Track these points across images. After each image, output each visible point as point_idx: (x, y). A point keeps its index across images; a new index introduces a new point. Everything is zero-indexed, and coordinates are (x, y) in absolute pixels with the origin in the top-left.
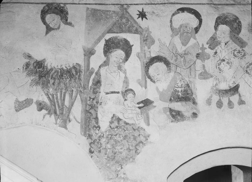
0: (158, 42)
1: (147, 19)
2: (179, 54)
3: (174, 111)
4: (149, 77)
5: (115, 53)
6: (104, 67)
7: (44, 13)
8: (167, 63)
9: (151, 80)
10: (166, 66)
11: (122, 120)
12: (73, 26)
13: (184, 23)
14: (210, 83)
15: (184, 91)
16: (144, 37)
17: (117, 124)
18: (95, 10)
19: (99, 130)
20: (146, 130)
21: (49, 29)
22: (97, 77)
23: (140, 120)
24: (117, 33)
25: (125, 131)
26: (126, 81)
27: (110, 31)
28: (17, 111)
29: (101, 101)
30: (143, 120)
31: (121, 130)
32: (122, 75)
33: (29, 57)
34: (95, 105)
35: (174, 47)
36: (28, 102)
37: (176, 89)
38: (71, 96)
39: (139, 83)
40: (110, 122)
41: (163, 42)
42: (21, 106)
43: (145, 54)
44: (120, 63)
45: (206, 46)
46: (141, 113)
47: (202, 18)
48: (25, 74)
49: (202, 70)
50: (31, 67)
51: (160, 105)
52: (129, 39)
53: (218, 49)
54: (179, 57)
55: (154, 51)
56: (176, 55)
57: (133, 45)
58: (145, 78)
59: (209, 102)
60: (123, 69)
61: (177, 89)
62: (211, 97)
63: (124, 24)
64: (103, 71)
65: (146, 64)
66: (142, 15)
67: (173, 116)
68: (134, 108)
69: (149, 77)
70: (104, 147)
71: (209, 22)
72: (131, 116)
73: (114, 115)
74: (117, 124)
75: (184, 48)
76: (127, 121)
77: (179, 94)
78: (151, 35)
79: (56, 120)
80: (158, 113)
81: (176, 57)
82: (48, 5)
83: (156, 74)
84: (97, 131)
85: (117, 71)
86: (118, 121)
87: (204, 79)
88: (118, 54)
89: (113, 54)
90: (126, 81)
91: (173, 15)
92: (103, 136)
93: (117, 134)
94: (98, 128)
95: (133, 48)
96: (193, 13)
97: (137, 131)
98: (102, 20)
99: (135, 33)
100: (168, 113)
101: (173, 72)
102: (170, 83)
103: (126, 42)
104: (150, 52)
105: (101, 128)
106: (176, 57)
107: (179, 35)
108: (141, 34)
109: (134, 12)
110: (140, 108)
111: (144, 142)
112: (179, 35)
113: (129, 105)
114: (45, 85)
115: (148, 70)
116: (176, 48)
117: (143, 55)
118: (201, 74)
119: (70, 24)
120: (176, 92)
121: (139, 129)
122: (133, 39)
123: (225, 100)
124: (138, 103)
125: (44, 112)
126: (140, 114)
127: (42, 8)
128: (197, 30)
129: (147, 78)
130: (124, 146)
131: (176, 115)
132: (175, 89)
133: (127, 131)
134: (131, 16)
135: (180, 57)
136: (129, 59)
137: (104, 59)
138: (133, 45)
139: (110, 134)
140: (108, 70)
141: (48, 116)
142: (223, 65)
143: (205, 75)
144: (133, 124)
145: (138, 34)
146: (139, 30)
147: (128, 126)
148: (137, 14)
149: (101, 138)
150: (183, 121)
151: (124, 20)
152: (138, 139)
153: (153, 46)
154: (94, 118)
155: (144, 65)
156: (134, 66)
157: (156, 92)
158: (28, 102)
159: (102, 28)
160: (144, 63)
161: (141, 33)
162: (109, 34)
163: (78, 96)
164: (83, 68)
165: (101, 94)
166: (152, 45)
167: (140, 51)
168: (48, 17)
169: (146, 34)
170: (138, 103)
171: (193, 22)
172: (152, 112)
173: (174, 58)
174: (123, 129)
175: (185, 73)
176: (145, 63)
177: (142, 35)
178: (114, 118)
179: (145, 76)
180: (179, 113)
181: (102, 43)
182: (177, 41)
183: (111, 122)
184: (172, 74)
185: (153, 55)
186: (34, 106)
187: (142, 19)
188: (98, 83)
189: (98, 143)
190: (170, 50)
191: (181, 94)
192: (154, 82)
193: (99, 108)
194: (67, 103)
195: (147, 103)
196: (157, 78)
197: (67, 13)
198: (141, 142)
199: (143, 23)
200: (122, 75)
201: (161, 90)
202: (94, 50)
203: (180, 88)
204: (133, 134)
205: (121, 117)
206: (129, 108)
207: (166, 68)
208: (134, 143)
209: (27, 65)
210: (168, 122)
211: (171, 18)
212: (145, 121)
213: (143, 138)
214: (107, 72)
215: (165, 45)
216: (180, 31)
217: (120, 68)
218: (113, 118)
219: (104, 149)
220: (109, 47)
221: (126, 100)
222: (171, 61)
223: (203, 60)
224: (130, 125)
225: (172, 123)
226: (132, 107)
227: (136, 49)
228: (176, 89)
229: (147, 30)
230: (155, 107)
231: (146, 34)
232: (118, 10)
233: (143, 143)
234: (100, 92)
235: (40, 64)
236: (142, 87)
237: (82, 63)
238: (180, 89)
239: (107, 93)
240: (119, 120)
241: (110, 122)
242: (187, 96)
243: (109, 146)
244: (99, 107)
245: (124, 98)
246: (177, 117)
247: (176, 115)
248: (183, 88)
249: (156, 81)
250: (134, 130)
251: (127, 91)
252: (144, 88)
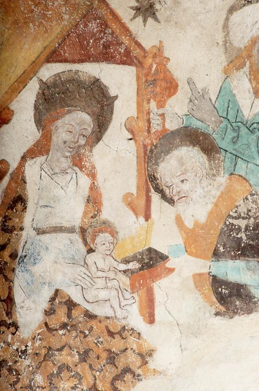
0: (187, 87)
1: (156, 20)
2: (245, 123)
3: (227, 284)
4: (158, 190)
5: (67, 118)
6: (35, 160)
8: (209, 148)
9: (164, 197)
10: (205, 157)
11: (79, 305)
15: (254, 229)
16: (147, 75)
17: (65, 320)
19: (13, 334)
20: (143, 335)
22: (13, 185)
23: (128, 308)
24: (74, 62)
25: (85, 336)
26: (94, 200)
27: (54, 56)
29: (24, 254)
30: (135, 309)
31: (74, 334)
32: (85, 181)
34: (6, 263)
35: (232, 102)
37: (231, 221)
40: (45, 311)
41: (200, 86)
43: (149, 121)
44: (79, 146)
46: (133, 286)
51: (185, 267)
52: (105, 81)
55: (176, 112)
56: (238, 125)
57: (116, 97)
58: (148, 191)
60: (88, 165)
61: (235, 222)
63: (94, 35)
64: (32, 170)
65: (151, 151)
67: (222, 299)
68: (111, 275)
69: (158, 190)
70: (27, 382)
72: (103, 294)
73: (57, 291)
74: (65, 320)
77: (239, 236)
78: (169, 66)
80: (179, 292)
81: (237, 130)
83: (177, 181)
84: (10, 336)
85: (69, 171)
86: (70, 310)
88: (78, 120)
89: (59, 123)
90: (94, 200)
91: (232, 10)
92: (26, 350)
93: (64, 347)
94: (12, 329)
95: (117, 103)
97: (117, 336)
98: (31, 25)
99: (123, 63)
100: (208, 288)
101: (227, 176)
102: (216, 205)
104: (163, 115)
105: (21, 329)
106: (237, 130)
107: (246, 69)
108: (139, 64)
111: (139, 371)
112: (246, 69)
113: (101, 265)
115: (156, 169)
116: (235, 103)
117: (142, 124)
120: (232, 230)
121: (122, 332)
122: (119, 80)
124: (126, 261)
126: (129, 290)
129: (152, 190)
130: (80, 379)
131: (230, 295)
132: (228, 223)
133: (91, 336)
134: (113, 13)
135: (247, 130)
136: (106, 137)
138: (116, 97)
139: (44, 344)
140: (45, 165)
144: (107, 318)
145: (129, 65)
146: (136, 52)
147: (93, 323)
148: (132, 8)
149: (20, 357)
150: (250, 312)
151: (93, 26)
152: (121, 363)
153: (174, 97)
154: (4, 301)
155: (145, 154)
157: (175, 228)
160: (145, 146)
161: (139, 62)
162: (49, 65)
165: (24, 233)
166: (170, 96)
167: (136, 116)
169: (155, 66)
170: (126, 261)
172: (162, 287)
173: (230, 135)
174: (81, 332)
176: (149, 148)
177: (143, 67)
178: (57, 301)
179: (147, 185)
180: (238, 291)
183: (49, 313)
184: (222, 179)
185: (172, 125)
187: (145, 21)
189: (10, 370)
190: (220, 111)
191: (246, 235)
192: (171, 201)
193: (17, 272)
196: (178, 189)
198: (127, 370)
200: (85, 181)
201: (189, 224)
202: (9, 109)
203: (243, 218)
204: (108, 347)
205: (77, 298)
206: (100, 274)
207: (207, 162)
208: (110, 372)
210: (207, 315)
211: (227, 19)
212: (141, 310)
213: (134, 359)
214: (43, 173)
215: (206, 97)
216: (250, 56)
217: (78, 161)
218: (53, 299)
219: (26, 388)
220: (52, 101)
221: (90, 251)
222: (223, 144)
224: (100, 322)
225: (218, 318)
226: (107, 269)
227: (125, 108)
228: (231, 221)
229: (158, 52)
230: (171, 270)
231: (155, 66)
233: (133, 374)
234: (22, 229)
236: (136, 215)
239: (40, 232)
240: (71, 305)
241: (45, 311)
243: (39, 379)
245: (86, 246)
246: (231, 303)
248: (252, 220)
249: (176, 198)
250: (111, 334)
252: (142, 219)
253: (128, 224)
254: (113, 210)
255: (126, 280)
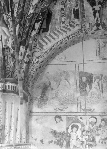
7: (55, 118)
12: (63, 121)
13: (92, 120)
14: (100, 137)
18: (69, 117)
21: (57, 122)
26: (77, 136)
27: (73, 123)
28: (49, 143)
33: (52, 129)
36: (52, 141)
38: (63, 140)
39: (81, 137)
42: (50, 142)
45: (98, 127)
47: (97, 119)
48: (51, 134)
49: (97, 133)
50: (53, 132)
51: (86, 142)
53: (102, 128)
54: (91, 130)
59: (99, 142)
62: (100, 140)
64: (71, 133)
66: (81, 118)
69: (83, 135)
71: (99, 120)
75: (92, 127)
76: (78, 147)
79: (59, 146)
82: (56, 116)
87: (98, 135)
88: (75, 129)
89: (73, 129)
90: (77, 136)
91: (90, 118)
96: (94, 118)
103: (77, 126)
108: (81, 123)
109: (79, 117)
110: (81, 143)
114: (56, 137)
118: (97, 134)
119: (62, 121)
122: (79, 125)
123: (104, 142)
124: (80, 142)
125: (56, 144)
127: (55, 117)
128: (96, 122)
137: (71, 130)
141: (57, 145)
142: (103, 132)
143: (98, 135)
156: (79, 132)
158: (52, 141)
159: (70, 122)
163: (65, 140)
164: (66, 133)
168: (57, 119)
171: (95, 120)
173: (90, 130)
175: (93, 134)
181: (71, 126)
182: (91, 125)
186: (54, 142)
188: (70, 136)
194: (62, 142)
195: (82, 142)
197: (61, 118)
199: (81, 121)
200: (76, 134)
209: (52, 132)
223: (98, 131)
227: (80, 128)
232: (75, 117)
235: (55, 131)
237: (66, 131)
238: (91, 138)
240: (75, 146)
242: (93, 140)
244: (70, 143)
247: (90, 145)
251: (77, 139)
253: (80, 138)
254: (79, 137)
255: (81, 144)
